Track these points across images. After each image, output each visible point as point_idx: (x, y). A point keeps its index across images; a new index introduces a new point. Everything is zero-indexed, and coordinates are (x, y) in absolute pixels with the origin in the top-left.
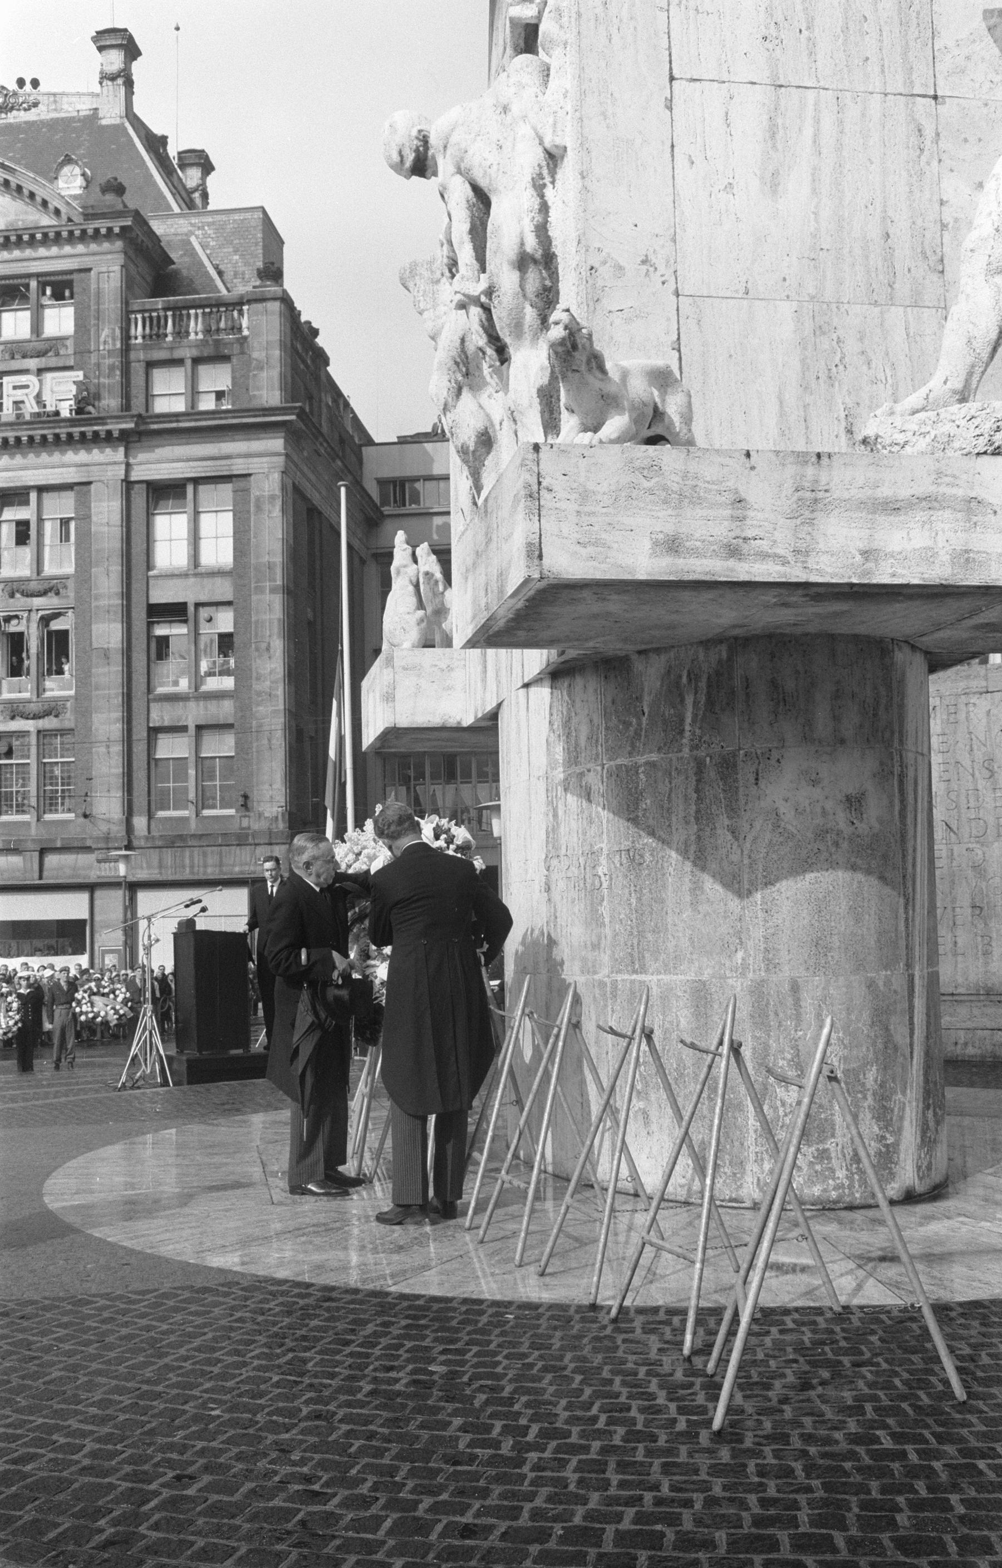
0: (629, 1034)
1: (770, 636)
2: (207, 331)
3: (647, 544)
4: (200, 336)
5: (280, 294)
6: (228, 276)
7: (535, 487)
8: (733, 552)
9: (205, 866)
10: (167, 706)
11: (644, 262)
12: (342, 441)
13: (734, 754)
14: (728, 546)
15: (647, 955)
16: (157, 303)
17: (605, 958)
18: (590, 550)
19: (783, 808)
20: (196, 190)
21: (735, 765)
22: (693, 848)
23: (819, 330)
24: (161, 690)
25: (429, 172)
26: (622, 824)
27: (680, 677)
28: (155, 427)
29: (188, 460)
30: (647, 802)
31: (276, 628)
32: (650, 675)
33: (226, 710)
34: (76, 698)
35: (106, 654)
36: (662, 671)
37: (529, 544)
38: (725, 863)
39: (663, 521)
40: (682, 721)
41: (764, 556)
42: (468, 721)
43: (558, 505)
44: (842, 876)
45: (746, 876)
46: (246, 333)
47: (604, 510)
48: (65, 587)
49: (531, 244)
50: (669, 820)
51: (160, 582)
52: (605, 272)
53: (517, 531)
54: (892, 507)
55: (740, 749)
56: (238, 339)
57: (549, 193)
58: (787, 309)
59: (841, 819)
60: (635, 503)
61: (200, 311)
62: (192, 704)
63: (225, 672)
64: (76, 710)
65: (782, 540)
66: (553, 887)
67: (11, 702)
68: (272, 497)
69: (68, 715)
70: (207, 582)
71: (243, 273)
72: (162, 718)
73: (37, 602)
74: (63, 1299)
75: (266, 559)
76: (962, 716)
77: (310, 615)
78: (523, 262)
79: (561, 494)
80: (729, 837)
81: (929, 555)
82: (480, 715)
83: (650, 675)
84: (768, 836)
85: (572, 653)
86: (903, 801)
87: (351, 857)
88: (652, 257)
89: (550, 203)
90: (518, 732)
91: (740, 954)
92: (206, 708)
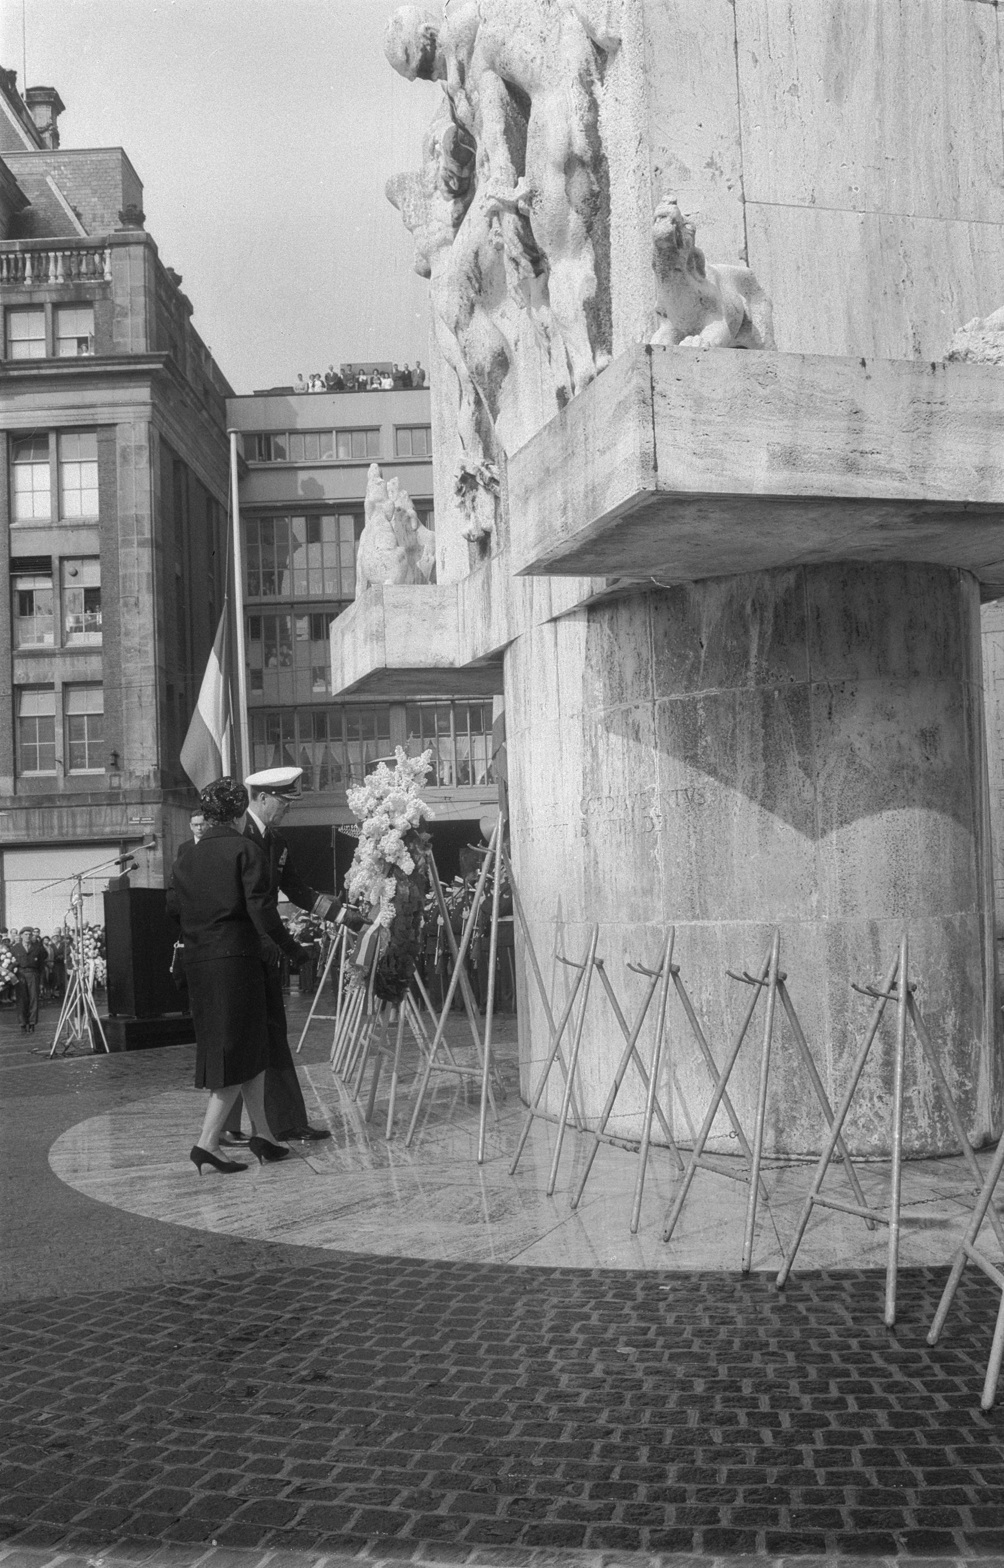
0: (760, 979)
1: (841, 564)
2: (68, 275)
3: (763, 457)
4: (61, 280)
5: (143, 238)
6: (87, 218)
7: (649, 392)
8: (851, 467)
9: (74, 826)
10: (31, 663)
11: (709, 165)
12: (206, 392)
13: (805, 687)
14: (845, 460)
15: (709, 900)
16: (14, 244)
17: (660, 905)
18: (709, 461)
20: (46, 129)
21: (806, 699)
22: (761, 786)
24: (24, 646)
25: (435, 75)
26: (678, 765)
27: (743, 607)
28: (15, 373)
29: (49, 409)
30: (708, 739)
31: (144, 582)
32: (709, 607)
33: (93, 667)
36: (723, 600)
37: (644, 454)
38: (797, 802)
40: (746, 653)
41: (881, 471)
42: (463, 659)
43: (672, 412)
44: (918, 813)
45: (820, 816)
46: (108, 277)
47: (720, 419)
49: (580, 144)
50: (734, 758)
51: (23, 534)
52: (670, 173)
53: (630, 441)
55: (811, 681)
56: (100, 284)
57: (598, 90)
58: (853, 220)
59: (917, 752)
60: (750, 412)
61: (59, 254)
62: (58, 661)
63: (92, 627)
65: (899, 457)
66: (592, 832)
68: (140, 448)
71: (102, 216)
72: (27, 675)
74: (153, 1289)
75: (133, 512)
77: (178, 568)
78: (570, 164)
79: (675, 400)
80: (801, 774)
82: (481, 654)
83: (709, 607)
84: (843, 773)
85: (626, 582)
86: (970, 736)
87: (372, 802)
88: (717, 160)
89: (599, 101)
90: (543, 669)
91: (815, 897)
92: (73, 665)
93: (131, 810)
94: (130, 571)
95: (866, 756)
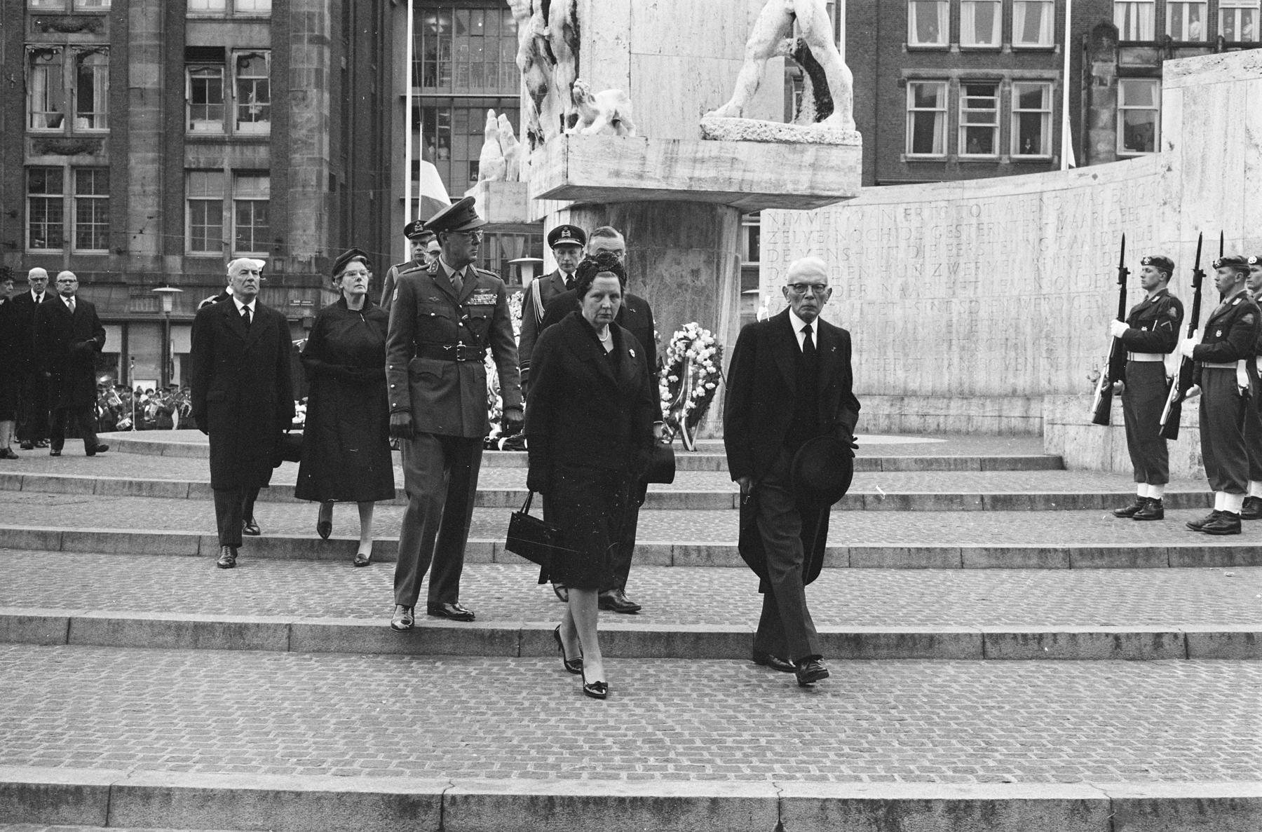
8: (641, 177)
10: (203, 149)
19: (666, 275)
23: (691, 70)
33: (261, 155)
34: (111, 136)
35: (142, 93)
39: (613, 165)
41: (651, 178)
48: (101, 25)
49: (569, 19)
51: (199, 25)
54: (703, 161)
58: (676, 60)
59: (688, 280)
62: (228, 149)
64: (110, 148)
65: (659, 173)
67: (44, 137)
69: (102, 153)
70: (245, 27)
73: (73, 38)
75: (306, 9)
76: (832, 220)
77: (343, 64)
81: (715, 180)
92: (242, 153)
93: (293, 294)
94: (301, 66)
95: (668, 279)
